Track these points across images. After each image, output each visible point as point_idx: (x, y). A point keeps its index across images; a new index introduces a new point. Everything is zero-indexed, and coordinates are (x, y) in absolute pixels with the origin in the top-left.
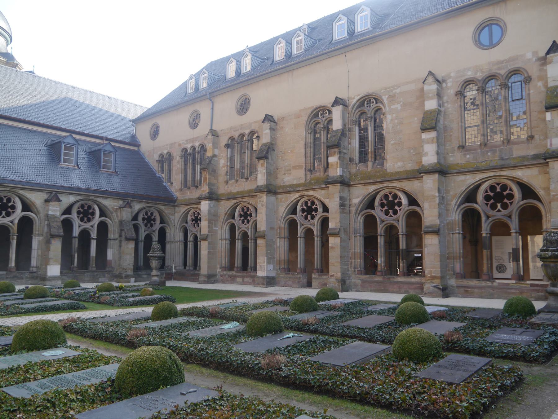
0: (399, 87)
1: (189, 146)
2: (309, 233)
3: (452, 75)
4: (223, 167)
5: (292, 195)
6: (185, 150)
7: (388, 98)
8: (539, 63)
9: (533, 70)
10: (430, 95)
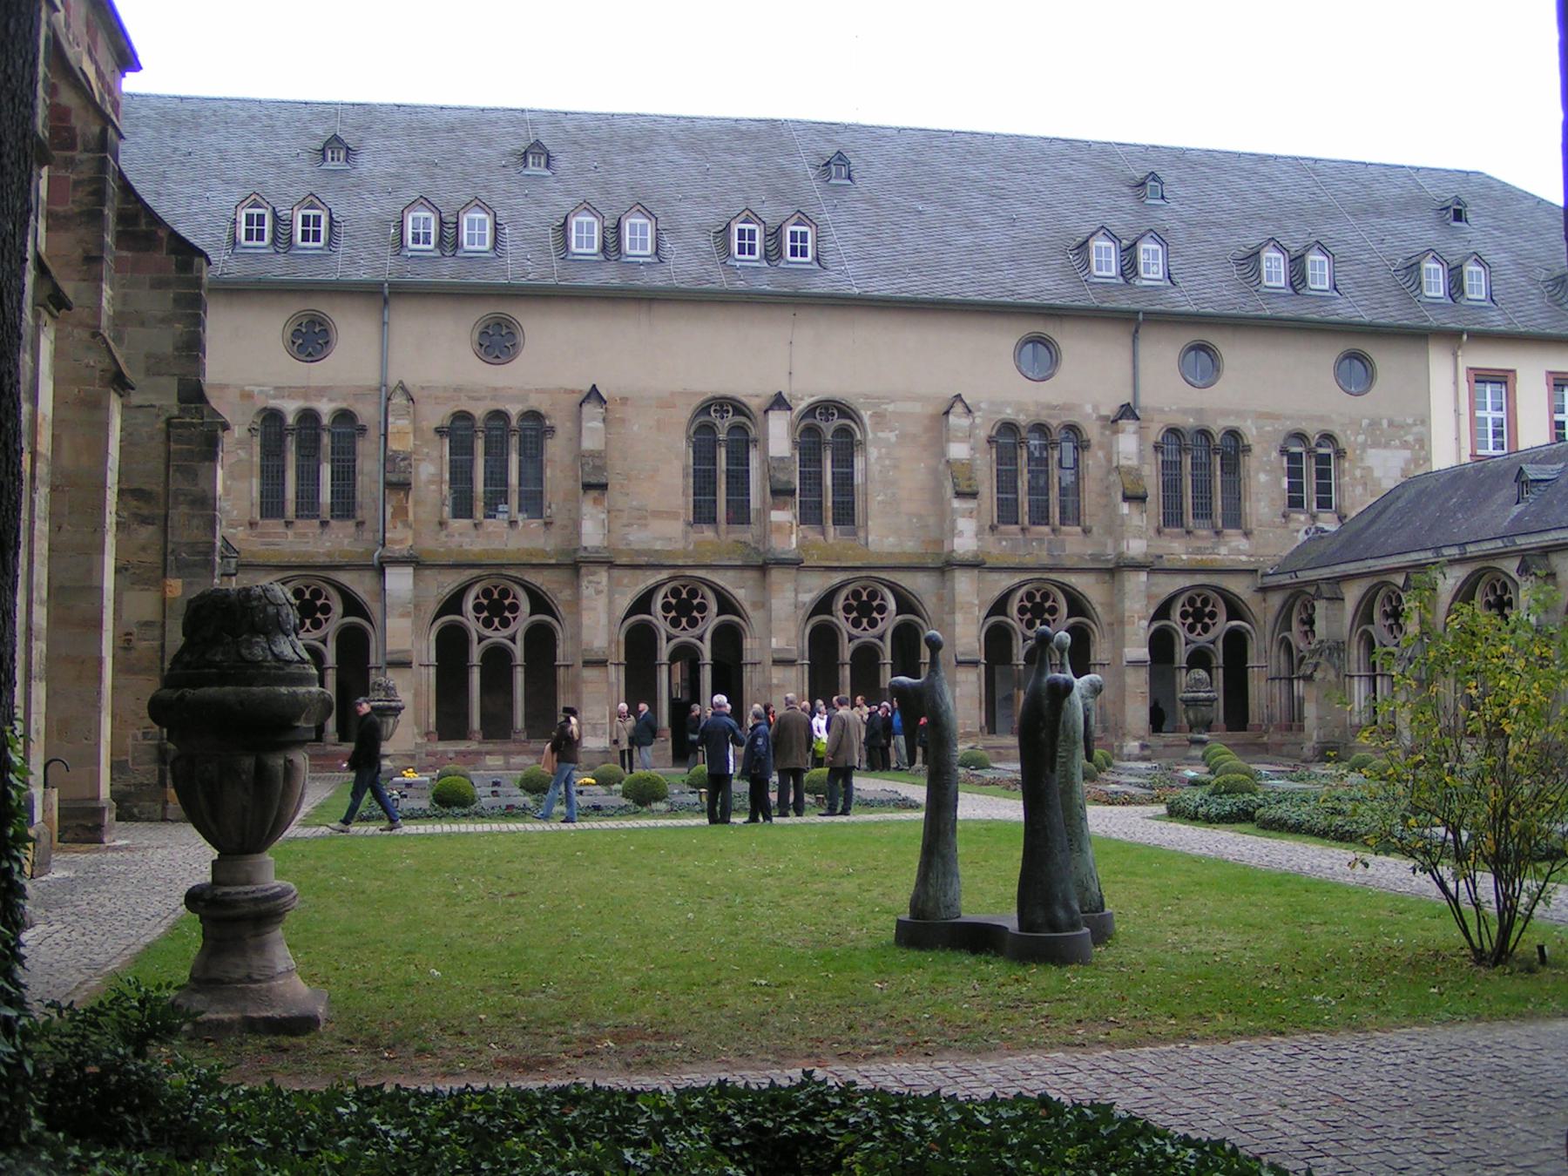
0: (893, 401)
1: (290, 408)
2: (686, 655)
3: (983, 406)
4: (430, 482)
5: (649, 573)
6: (272, 417)
7: (871, 416)
8: (1098, 423)
9: (1092, 431)
10: (960, 435)
